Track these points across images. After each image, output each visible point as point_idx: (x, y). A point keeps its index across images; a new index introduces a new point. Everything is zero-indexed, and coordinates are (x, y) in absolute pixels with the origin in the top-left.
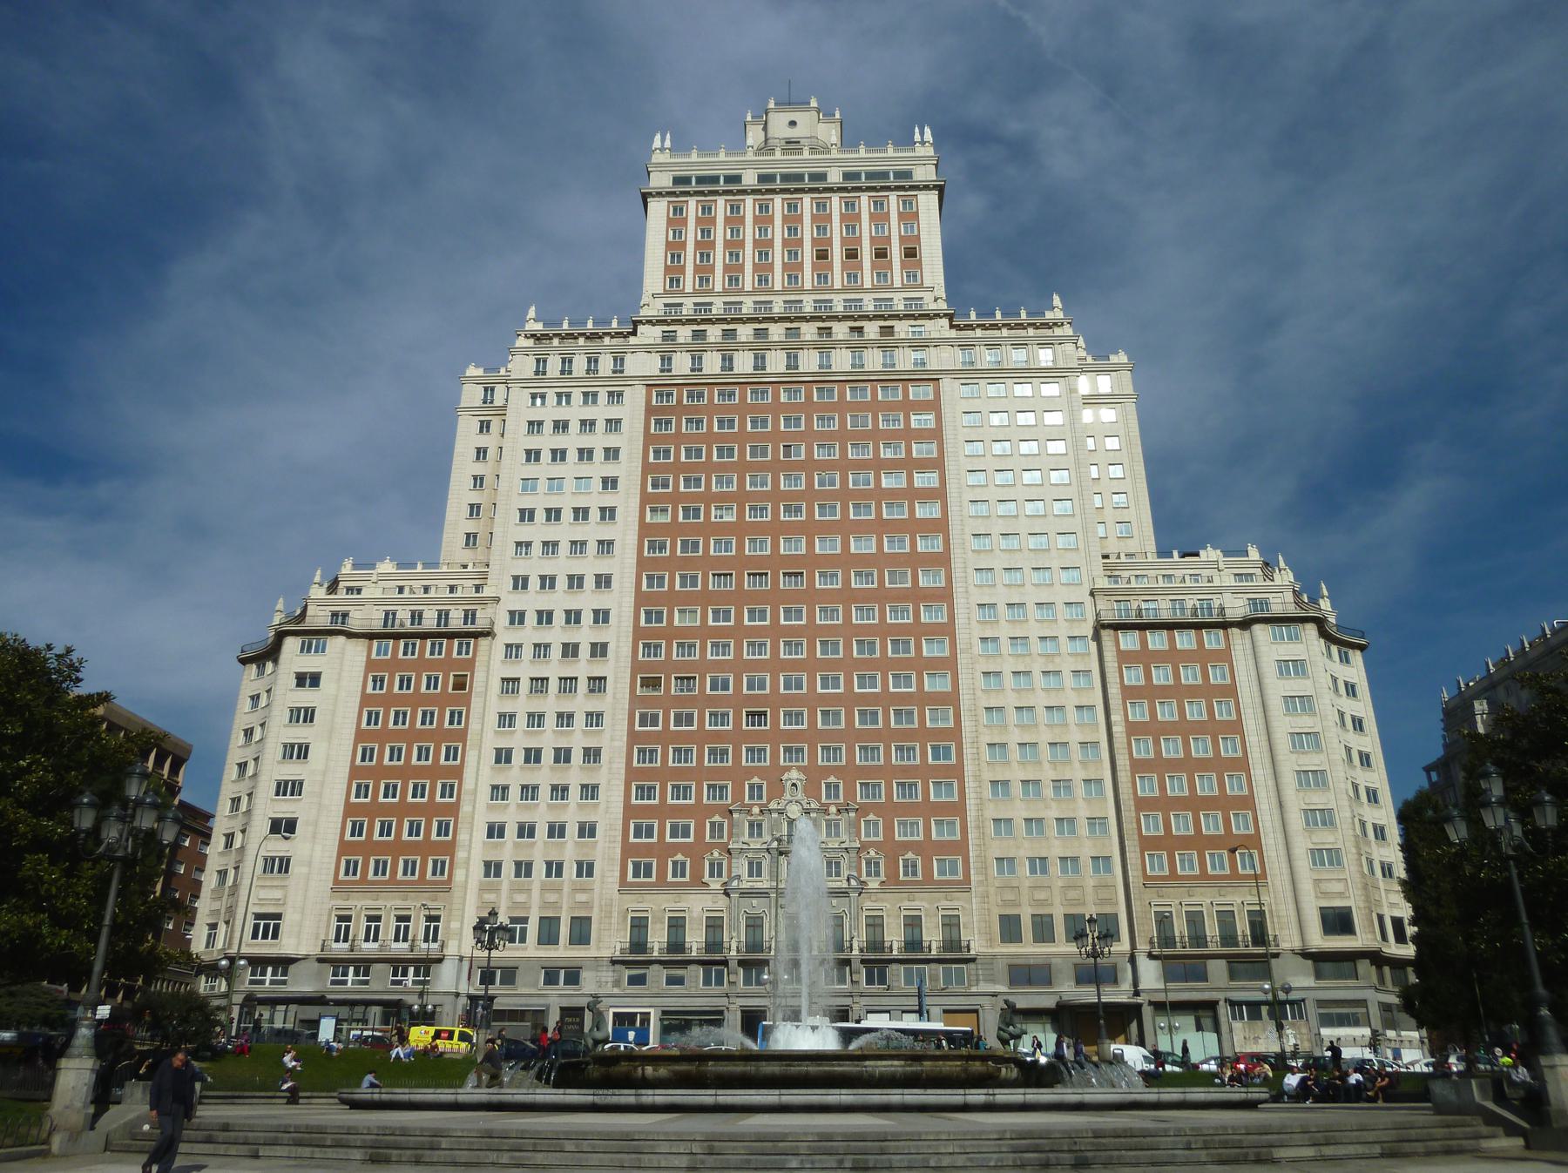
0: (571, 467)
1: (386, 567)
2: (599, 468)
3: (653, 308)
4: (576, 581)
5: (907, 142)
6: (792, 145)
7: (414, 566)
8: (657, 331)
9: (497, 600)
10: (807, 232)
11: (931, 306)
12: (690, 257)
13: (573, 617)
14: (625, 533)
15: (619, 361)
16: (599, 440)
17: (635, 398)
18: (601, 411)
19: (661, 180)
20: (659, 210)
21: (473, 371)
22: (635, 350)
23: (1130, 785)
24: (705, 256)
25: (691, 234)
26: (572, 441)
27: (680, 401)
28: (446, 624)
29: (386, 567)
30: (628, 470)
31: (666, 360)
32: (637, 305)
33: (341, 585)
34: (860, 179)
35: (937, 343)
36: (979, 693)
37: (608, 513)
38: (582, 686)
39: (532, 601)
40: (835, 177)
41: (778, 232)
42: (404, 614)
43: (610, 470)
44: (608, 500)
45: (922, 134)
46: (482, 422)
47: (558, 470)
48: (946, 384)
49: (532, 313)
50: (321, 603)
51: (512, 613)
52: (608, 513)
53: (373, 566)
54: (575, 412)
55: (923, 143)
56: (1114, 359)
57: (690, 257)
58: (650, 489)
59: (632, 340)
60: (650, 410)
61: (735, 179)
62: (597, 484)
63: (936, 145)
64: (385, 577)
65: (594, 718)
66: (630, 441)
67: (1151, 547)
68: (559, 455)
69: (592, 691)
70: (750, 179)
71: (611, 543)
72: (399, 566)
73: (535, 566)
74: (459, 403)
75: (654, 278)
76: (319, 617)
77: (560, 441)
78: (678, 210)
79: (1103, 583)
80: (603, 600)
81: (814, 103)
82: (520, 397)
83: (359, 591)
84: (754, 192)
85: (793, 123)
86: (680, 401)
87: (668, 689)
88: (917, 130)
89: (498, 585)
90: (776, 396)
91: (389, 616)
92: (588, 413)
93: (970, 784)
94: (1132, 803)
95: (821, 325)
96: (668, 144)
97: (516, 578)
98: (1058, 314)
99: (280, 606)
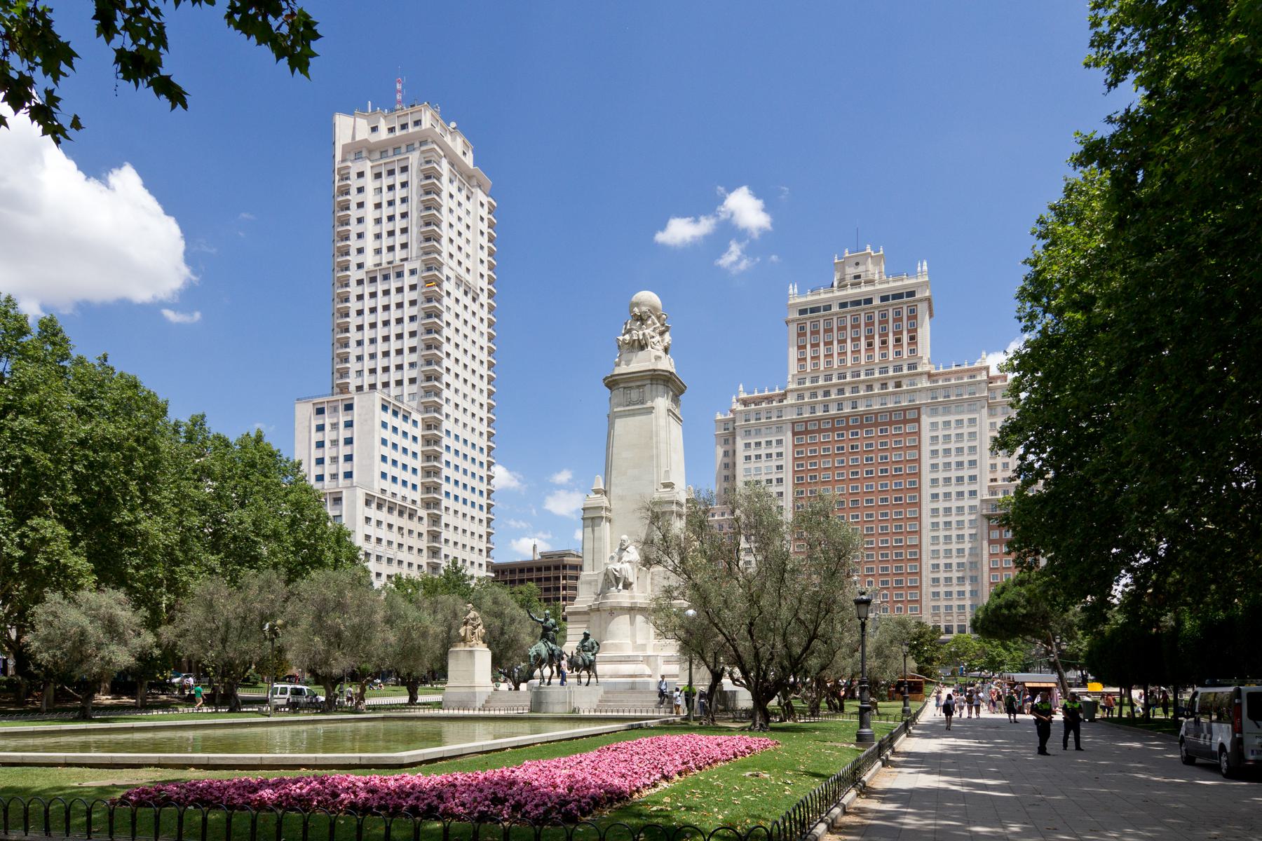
0: (763, 464)
2: (774, 463)
8: (795, 394)
16: (774, 450)
26: (763, 451)
30: (787, 462)
37: (780, 481)
45: (922, 266)
48: (923, 410)
49: (741, 388)
52: (780, 481)
55: (922, 272)
59: (785, 402)
62: (774, 469)
63: (929, 273)
78: (802, 328)
84: (837, 314)
85: (857, 264)
86: (806, 428)
90: (847, 422)
96: (796, 290)
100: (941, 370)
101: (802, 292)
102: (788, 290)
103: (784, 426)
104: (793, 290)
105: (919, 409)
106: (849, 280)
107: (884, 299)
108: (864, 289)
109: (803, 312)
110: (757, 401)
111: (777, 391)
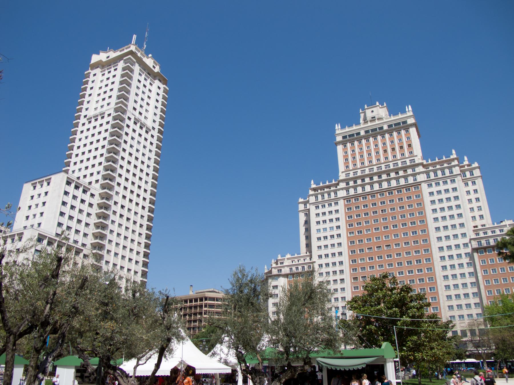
0: (328, 225)
1: (288, 256)
3: (342, 176)
4: (334, 255)
5: (404, 112)
6: (373, 119)
7: (294, 255)
9: (315, 262)
10: (380, 145)
11: (417, 162)
12: (350, 159)
13: (334, 264)
14: (344, 240)
15: (336, 193)
17: (341, 202)
18: (333, 208)
19: (339, 139)
20: (340, 148)
21: (301, 200)
22: (339, 190)
23: (485, 293)
24: (354, 158)
25: (350, 152)
27: (352, 202)
28: (304, 270)
29: (288, 256)
30: (342, 223)
31: (348, 191)
32: (338, 176)
33: (279, 262)
34: (392, 127)
35: (419, 173)
36: (441, 272)
38: (339, 281)
39: (324, 261)
40: (385, 127)
41: (372, 147)
42: (294, 268)
43: (338, 224)
44: (339, 232)
45: (408, 108)
46: (305, 214)
47: (325, 226)
50: (275, 268)
51: (319, 265)
52: (339, 235)
53: (285, 256)
54: (327, 209)
55: (409, 111)
56: (473, 166)
57: (350, 159)
58: (348, 227)
59: (338, 187)
60: (345, 205)
61: (358, 134)
64: (288, 259)
65: (343, 289)
66: (342, 215)
67: (490, 221)
68: (325, 222)
69: (341, 282)
70: (362, 133)
71: (341, 243)
72: (292, 255)
73: (323, 252)
74: (298, 209)
75: (342, 167)
76: (275, 272)
77: (324, 218)
78: (345, 146)
79: (474, 236)
80: (340, 259)
81: (377, 104)
82: (312, 208)
83: (283, 263)
85: (372, 111)
87: (360, 280)
88: (407, 107)
89: (315, 258)
90: (377, 196)
91: (291, 269)
92: (330, 209)
93: (441, 297)
94: (486, 298)
95: (387, 173)
96: (339, 127)
97: (319, 256)
98: (454, 156)
99: (266, 268)
100: (430, 162)
101: (343, 127)
102: (335, 127)
103: (339, 202)
104: (338, 127)
105: (420, 185)
106: (369, 119)
107: (390, 126)
108: (377, 122)
109: (344, 137)
110: (322, 188)
111: (334, 182)
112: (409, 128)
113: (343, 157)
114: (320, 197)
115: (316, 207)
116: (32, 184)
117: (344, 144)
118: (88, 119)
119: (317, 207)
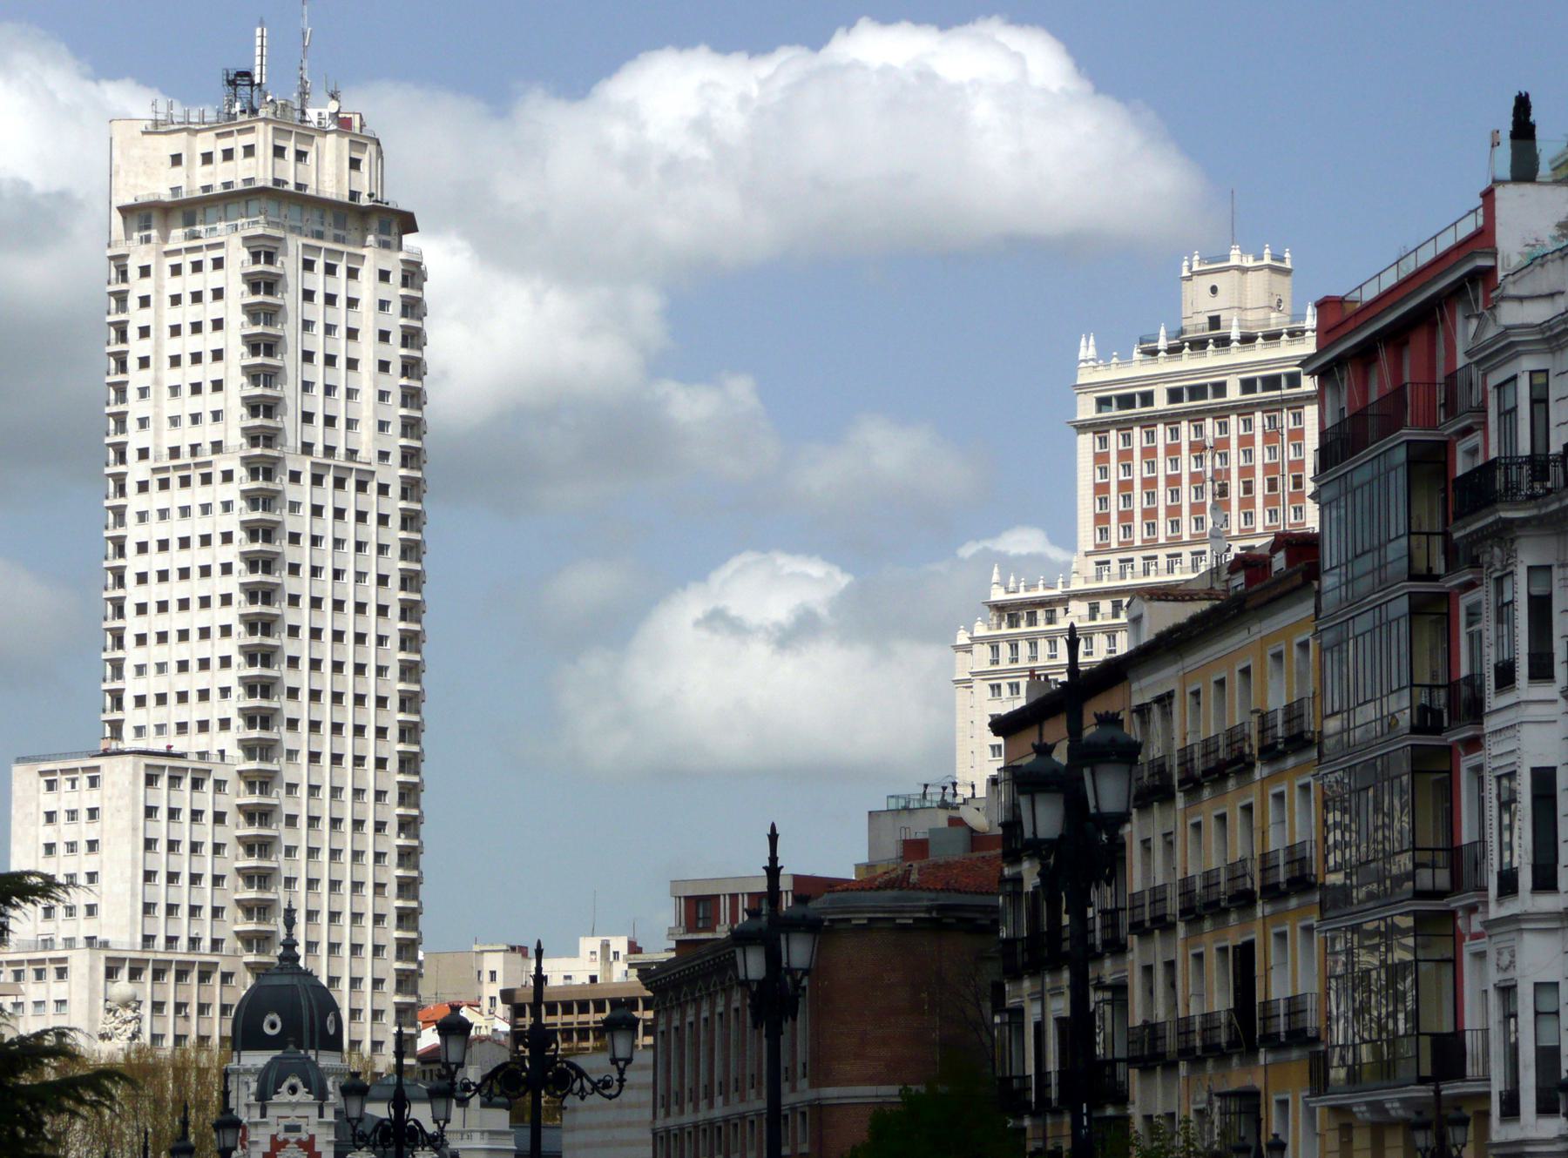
19: (1086, 410)
78: (1104, 442)
85: (1214, 290)
96: (1092, 353)
101: (1103, 356)
102: (1078, 350)
104: (1087, 350)
109: (1103, 403)
112: (1302, 407)
113: (1091, 491)
114: (1005, 649)
115: (992, 687)
116: (42, 773)
117: (1098, 428)
118: (155, 471)
119: (996, 689)
